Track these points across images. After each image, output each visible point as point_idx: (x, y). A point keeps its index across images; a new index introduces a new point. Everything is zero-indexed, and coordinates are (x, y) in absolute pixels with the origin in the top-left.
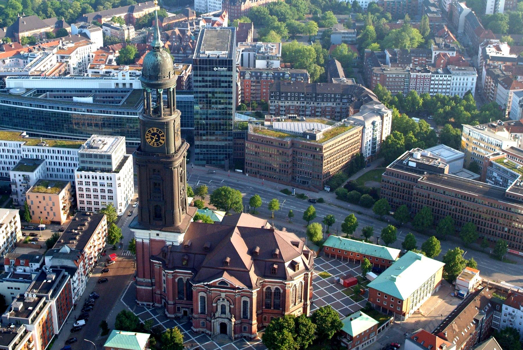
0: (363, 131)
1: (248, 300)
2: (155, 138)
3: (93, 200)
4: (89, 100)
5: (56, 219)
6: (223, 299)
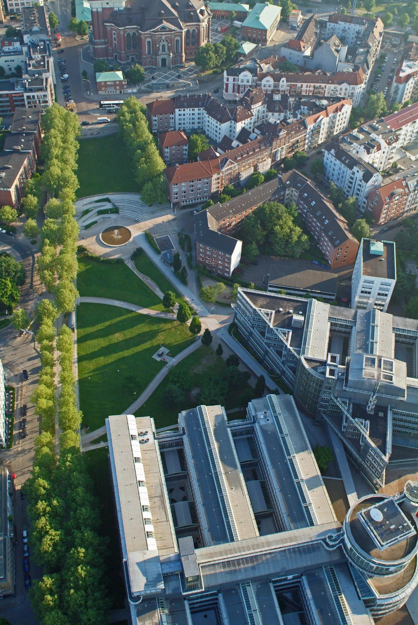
1: (179, 38)
6: (163, 41)
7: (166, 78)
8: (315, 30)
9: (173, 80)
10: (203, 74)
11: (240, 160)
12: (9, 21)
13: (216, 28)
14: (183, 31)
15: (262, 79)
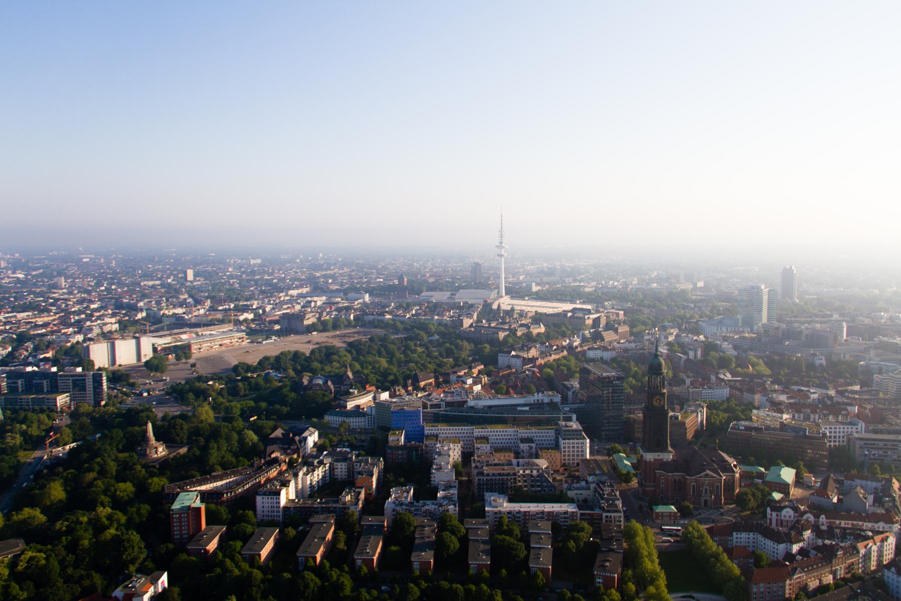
0: (697, 416)
1: (719, 484)
2: (659, 401)
4: (527, 408)
8: (835, 485)
11: (806, 571)
15: (803, 515)
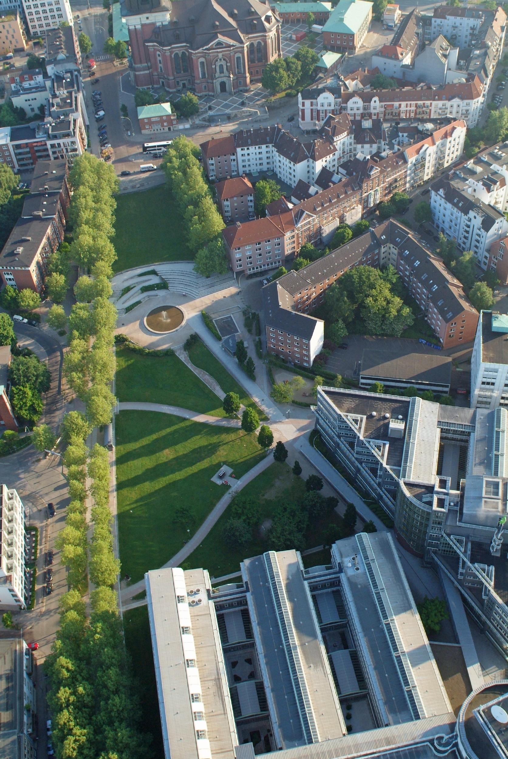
1: (240, 55)
3: (43, 22)
5: (19, 46)
6: (220, 60)
7: (227, 106)
8: (416, 30)
9: (235, 108)
10: (273, 99)
11: (320, 211)
12: (31, 48)
13: (289, 36)
14: (245, 45)
15: (348, 100)
